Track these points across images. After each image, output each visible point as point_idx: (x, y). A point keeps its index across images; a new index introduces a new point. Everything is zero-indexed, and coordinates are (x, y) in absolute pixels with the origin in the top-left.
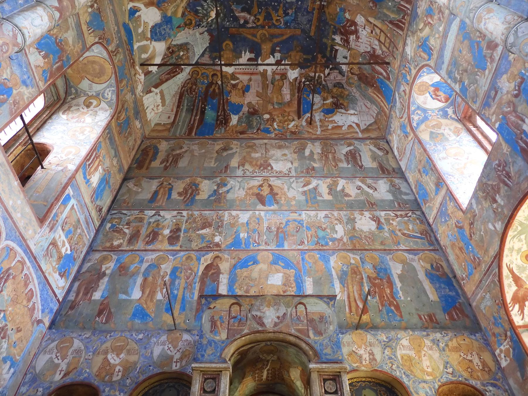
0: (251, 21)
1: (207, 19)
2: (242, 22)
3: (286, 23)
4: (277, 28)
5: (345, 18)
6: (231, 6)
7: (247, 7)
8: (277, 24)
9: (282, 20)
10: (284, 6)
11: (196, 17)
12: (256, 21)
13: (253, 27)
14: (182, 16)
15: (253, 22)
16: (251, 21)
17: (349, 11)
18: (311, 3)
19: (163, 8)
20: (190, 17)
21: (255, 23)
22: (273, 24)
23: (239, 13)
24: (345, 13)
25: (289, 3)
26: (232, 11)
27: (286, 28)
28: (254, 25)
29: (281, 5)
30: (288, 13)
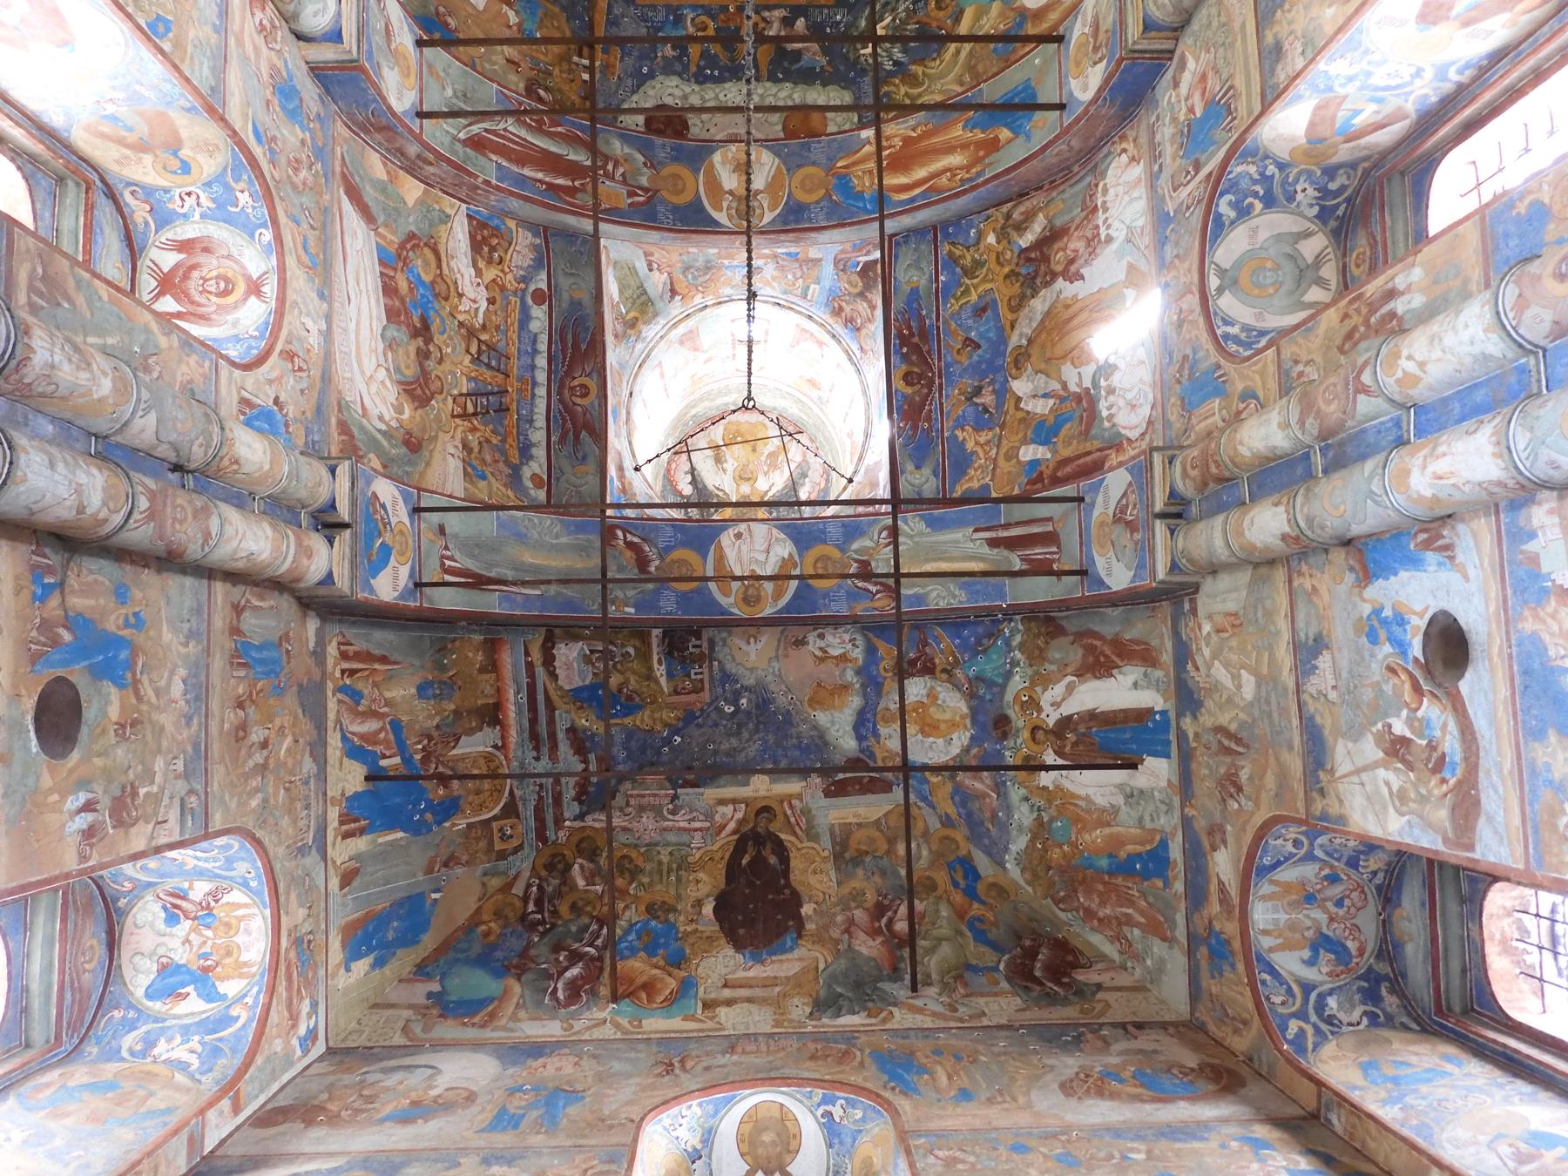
0: (776, 25)
1: (894, 20)
2: (800, 24)
3: (679, 20)
4: (702, 6)
5: (517, 12)
6: (829, 63)
7: (786, 64)
8: (703, 18)
9: (691, 30)
10: (686, 67)
11: (925, 20)
12: (762, 25)
13: (770, 8)
14: (962, 12)
15: (768, 22)
16: (776, 25)
17: (510, 27)
18: (614, 66)
19: (1012, 14)
20: (941, 14)
21: (764, 19)
22: (713, 18)
23: (807, 49)
24: (519, 25)
25: (675, 73)
26: (825, 51)
27: (679, 7)
28: (766, 14)
29: (693, 69)
30: (674, 48)
